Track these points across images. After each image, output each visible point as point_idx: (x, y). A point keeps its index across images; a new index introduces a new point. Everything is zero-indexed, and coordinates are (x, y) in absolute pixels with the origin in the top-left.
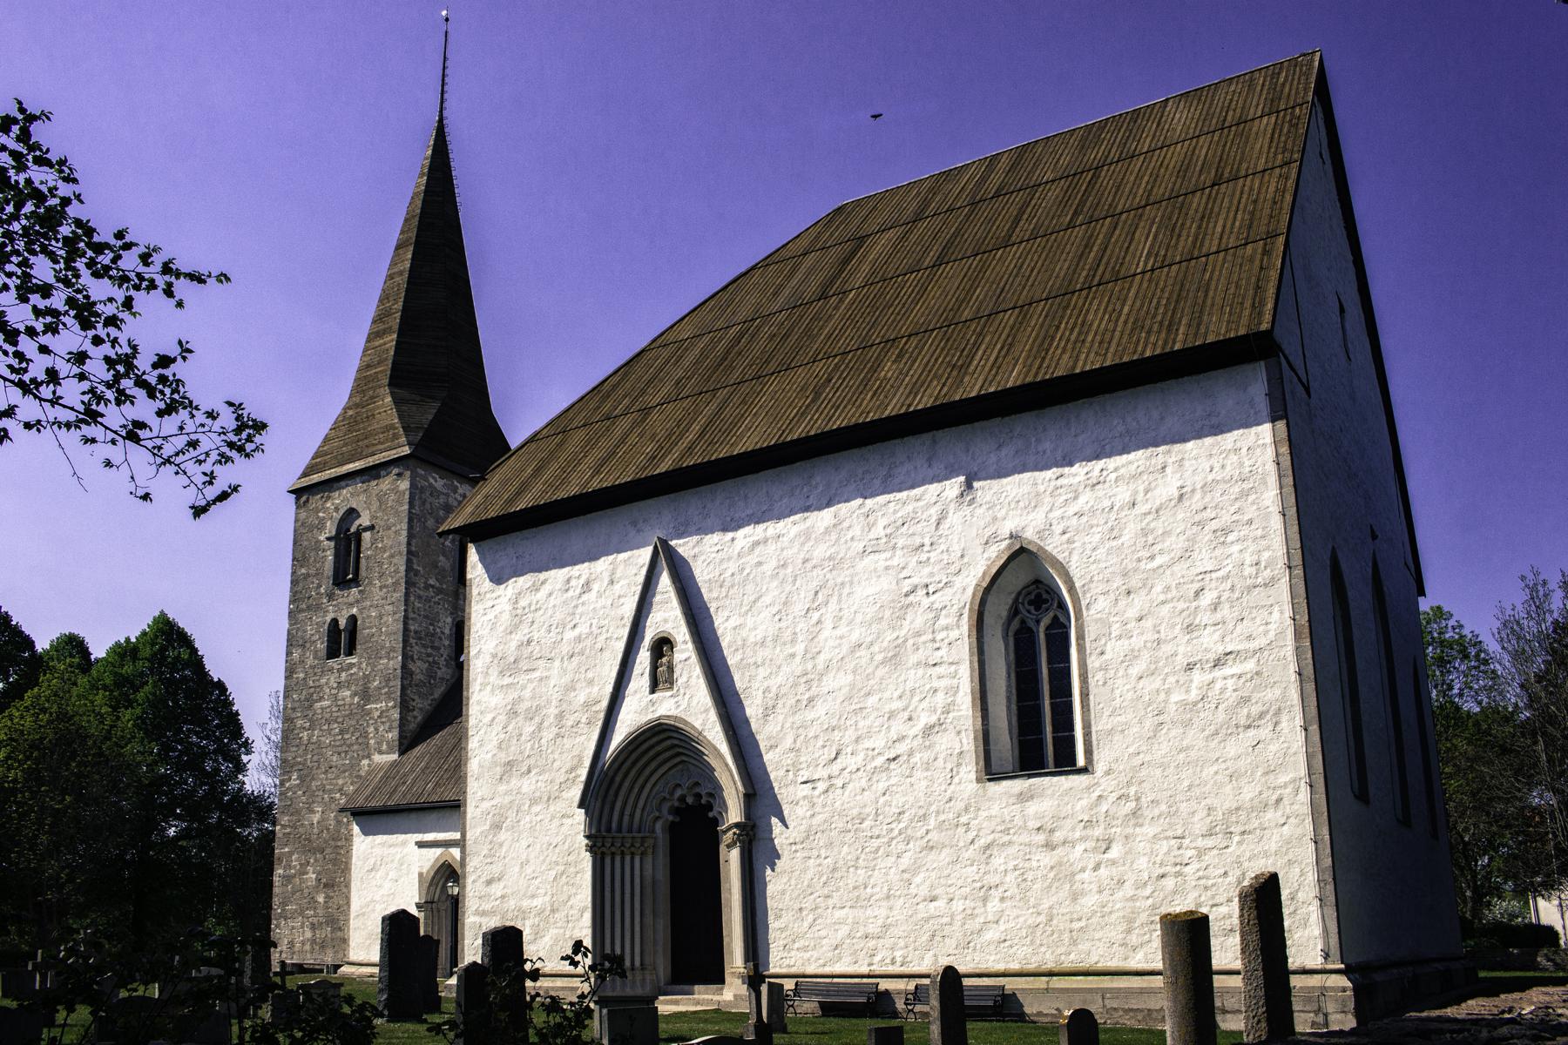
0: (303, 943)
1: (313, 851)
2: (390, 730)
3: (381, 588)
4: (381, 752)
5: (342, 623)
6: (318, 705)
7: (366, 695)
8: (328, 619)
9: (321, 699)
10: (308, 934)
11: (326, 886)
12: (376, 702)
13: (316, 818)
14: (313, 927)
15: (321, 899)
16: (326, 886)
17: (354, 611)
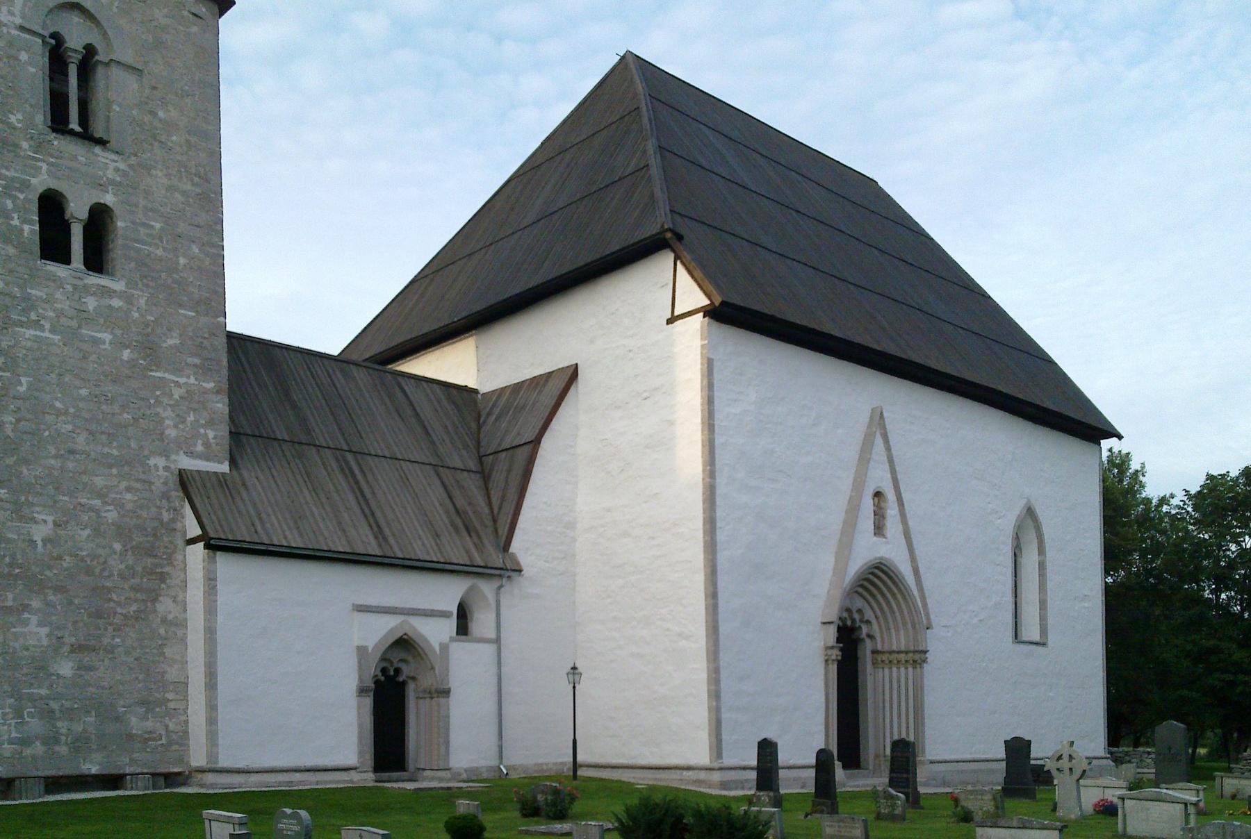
0: (25, 742)
1: (36, 585)
2: (211, 423)
3: (170, 188)
4: (190, 454)
5: (78, 209)
6: (30, 333)
7: (150, 350)
8: (42, 181)
9: (37, 324)
10: (35, 725)
11: (77, 649)
12: (178, 371)
13: (39, 533)
14: (48, 715)
15: (66, 668)
16: (77, 649)
17: (109, 199)
